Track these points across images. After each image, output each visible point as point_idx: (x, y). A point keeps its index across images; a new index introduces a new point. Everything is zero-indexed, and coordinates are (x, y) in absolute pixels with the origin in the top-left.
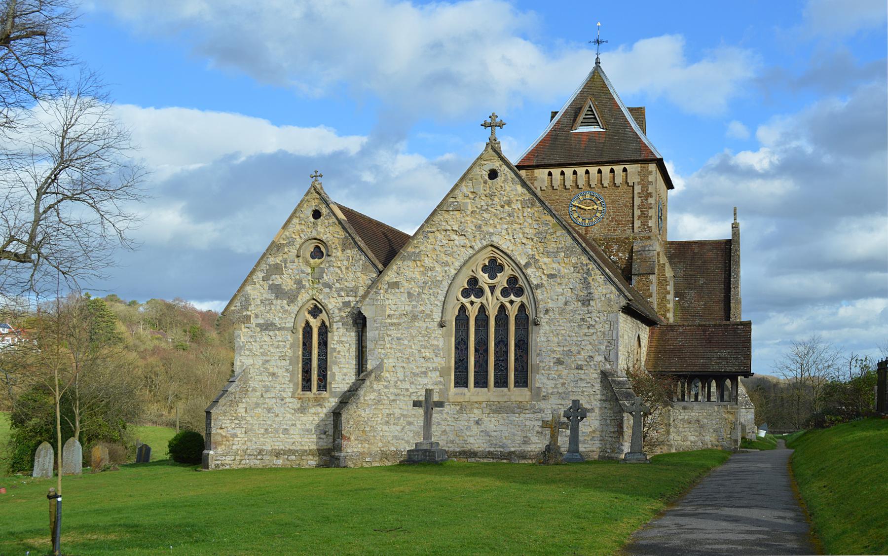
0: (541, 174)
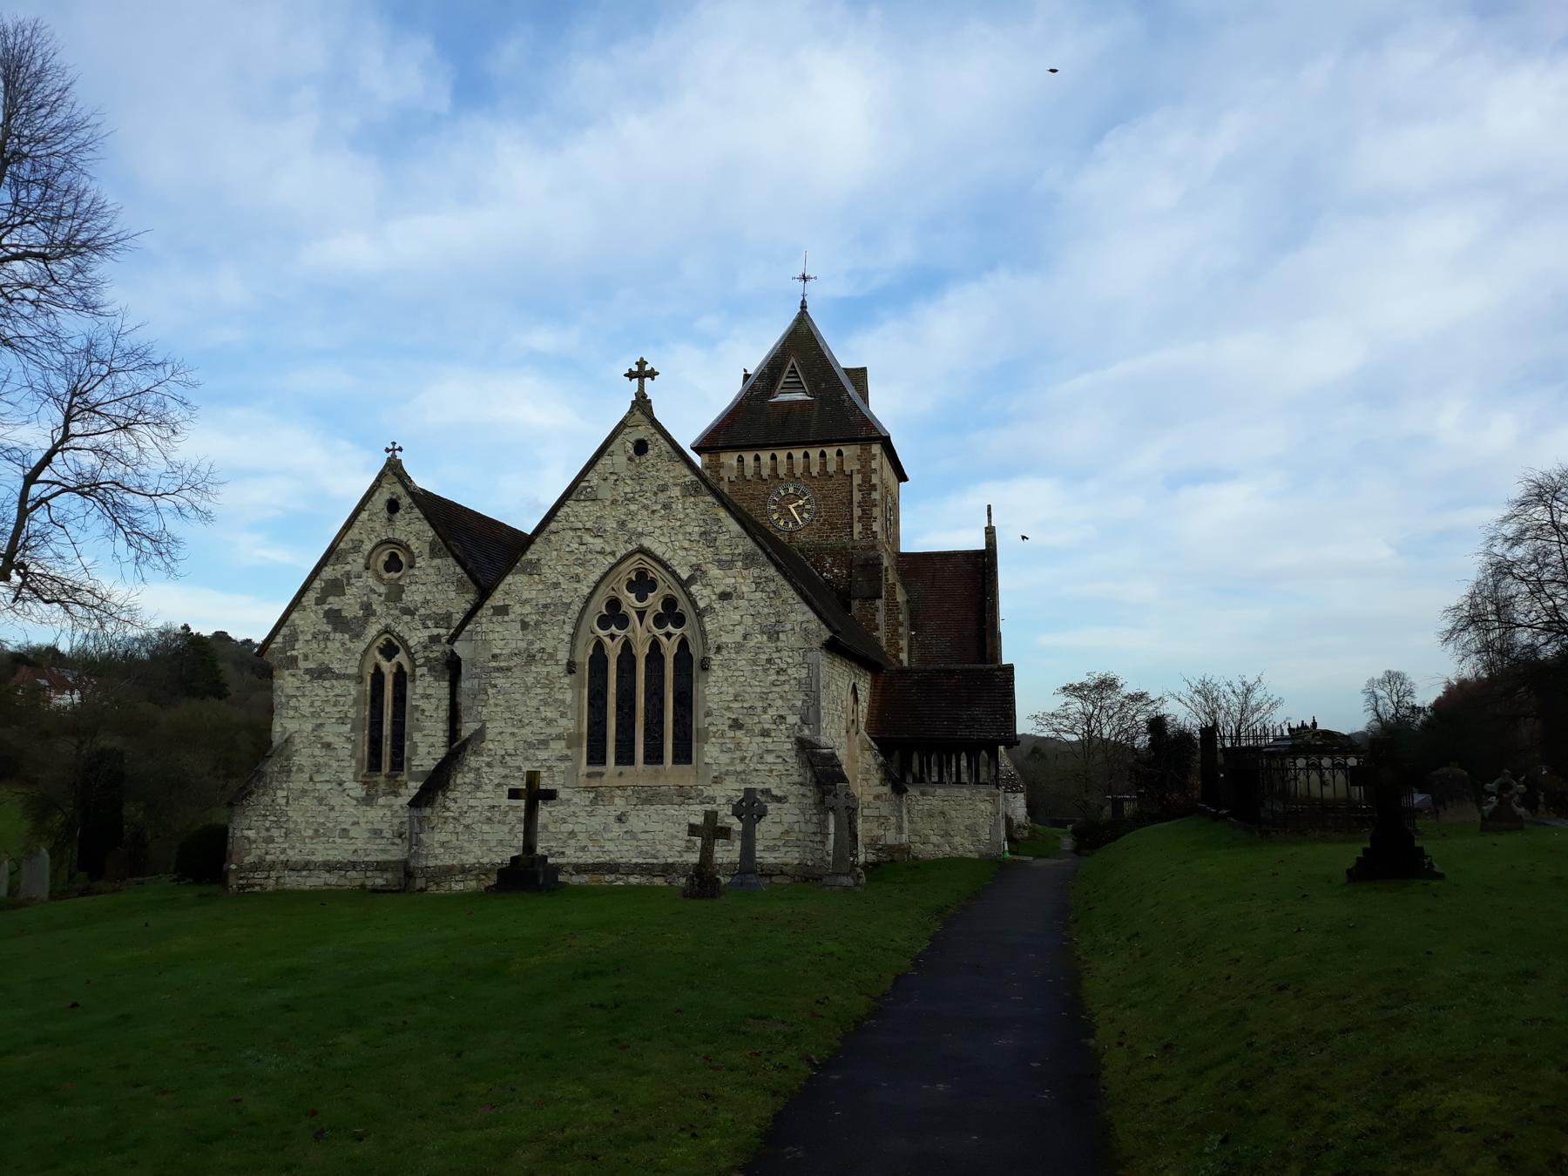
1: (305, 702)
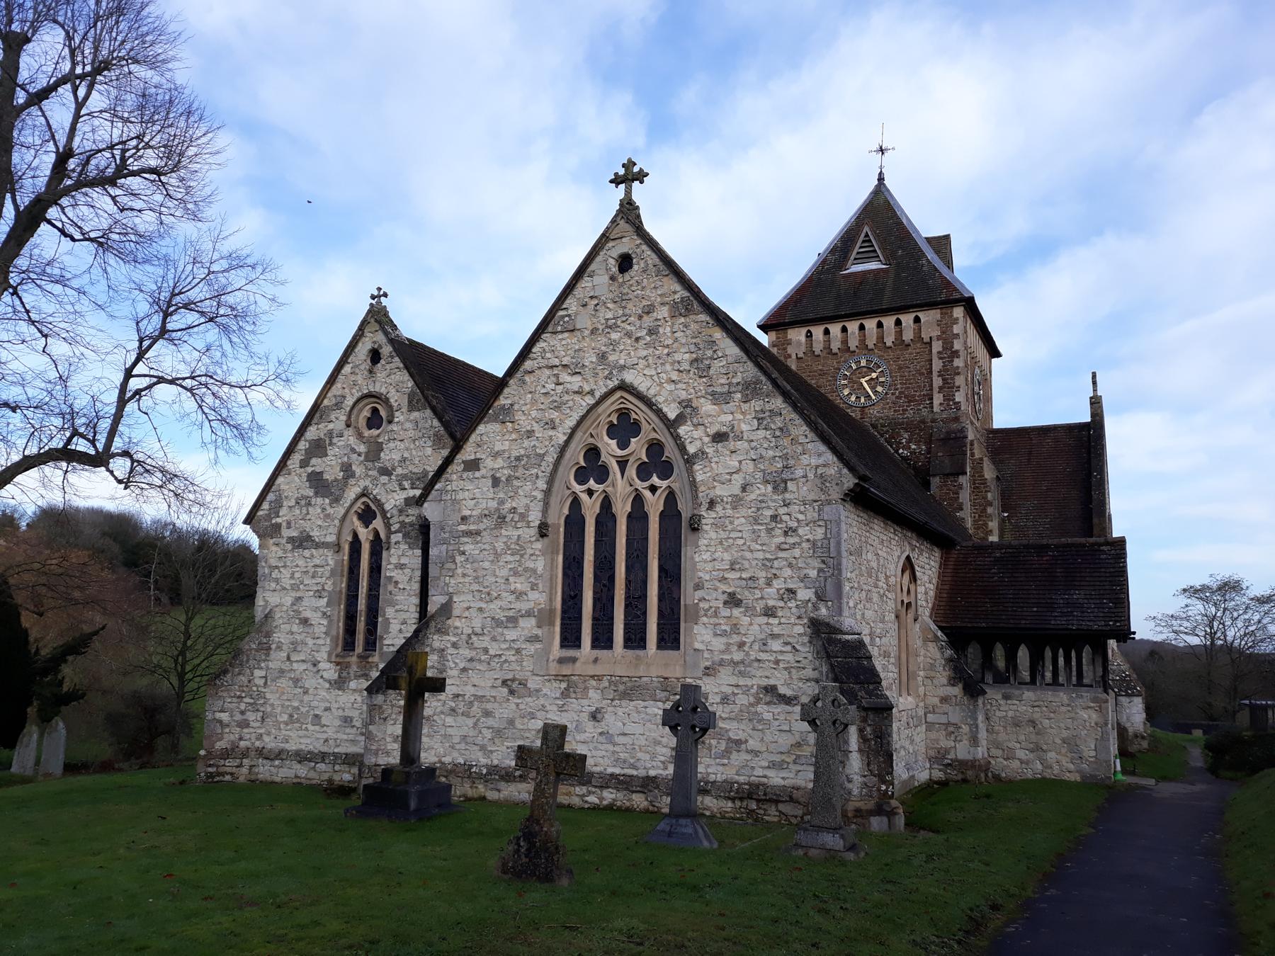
0: (797, 335)
1: (286, 573)
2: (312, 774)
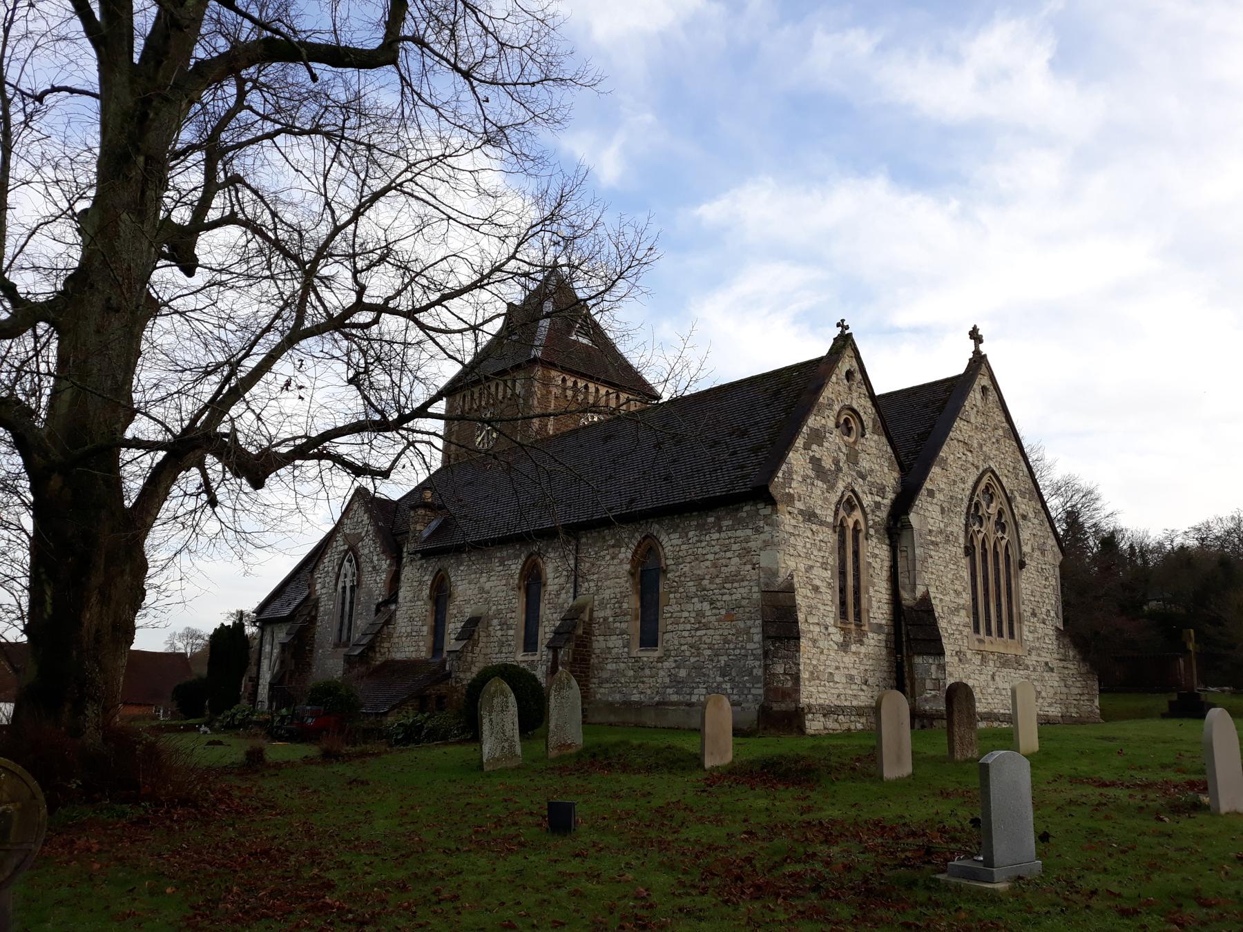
2: (836, 726)
